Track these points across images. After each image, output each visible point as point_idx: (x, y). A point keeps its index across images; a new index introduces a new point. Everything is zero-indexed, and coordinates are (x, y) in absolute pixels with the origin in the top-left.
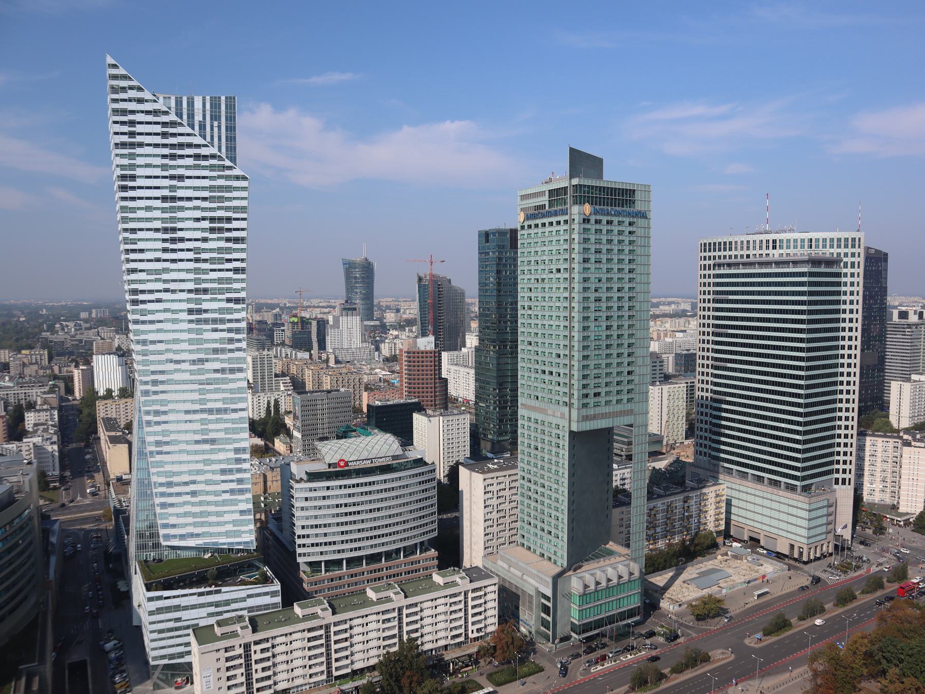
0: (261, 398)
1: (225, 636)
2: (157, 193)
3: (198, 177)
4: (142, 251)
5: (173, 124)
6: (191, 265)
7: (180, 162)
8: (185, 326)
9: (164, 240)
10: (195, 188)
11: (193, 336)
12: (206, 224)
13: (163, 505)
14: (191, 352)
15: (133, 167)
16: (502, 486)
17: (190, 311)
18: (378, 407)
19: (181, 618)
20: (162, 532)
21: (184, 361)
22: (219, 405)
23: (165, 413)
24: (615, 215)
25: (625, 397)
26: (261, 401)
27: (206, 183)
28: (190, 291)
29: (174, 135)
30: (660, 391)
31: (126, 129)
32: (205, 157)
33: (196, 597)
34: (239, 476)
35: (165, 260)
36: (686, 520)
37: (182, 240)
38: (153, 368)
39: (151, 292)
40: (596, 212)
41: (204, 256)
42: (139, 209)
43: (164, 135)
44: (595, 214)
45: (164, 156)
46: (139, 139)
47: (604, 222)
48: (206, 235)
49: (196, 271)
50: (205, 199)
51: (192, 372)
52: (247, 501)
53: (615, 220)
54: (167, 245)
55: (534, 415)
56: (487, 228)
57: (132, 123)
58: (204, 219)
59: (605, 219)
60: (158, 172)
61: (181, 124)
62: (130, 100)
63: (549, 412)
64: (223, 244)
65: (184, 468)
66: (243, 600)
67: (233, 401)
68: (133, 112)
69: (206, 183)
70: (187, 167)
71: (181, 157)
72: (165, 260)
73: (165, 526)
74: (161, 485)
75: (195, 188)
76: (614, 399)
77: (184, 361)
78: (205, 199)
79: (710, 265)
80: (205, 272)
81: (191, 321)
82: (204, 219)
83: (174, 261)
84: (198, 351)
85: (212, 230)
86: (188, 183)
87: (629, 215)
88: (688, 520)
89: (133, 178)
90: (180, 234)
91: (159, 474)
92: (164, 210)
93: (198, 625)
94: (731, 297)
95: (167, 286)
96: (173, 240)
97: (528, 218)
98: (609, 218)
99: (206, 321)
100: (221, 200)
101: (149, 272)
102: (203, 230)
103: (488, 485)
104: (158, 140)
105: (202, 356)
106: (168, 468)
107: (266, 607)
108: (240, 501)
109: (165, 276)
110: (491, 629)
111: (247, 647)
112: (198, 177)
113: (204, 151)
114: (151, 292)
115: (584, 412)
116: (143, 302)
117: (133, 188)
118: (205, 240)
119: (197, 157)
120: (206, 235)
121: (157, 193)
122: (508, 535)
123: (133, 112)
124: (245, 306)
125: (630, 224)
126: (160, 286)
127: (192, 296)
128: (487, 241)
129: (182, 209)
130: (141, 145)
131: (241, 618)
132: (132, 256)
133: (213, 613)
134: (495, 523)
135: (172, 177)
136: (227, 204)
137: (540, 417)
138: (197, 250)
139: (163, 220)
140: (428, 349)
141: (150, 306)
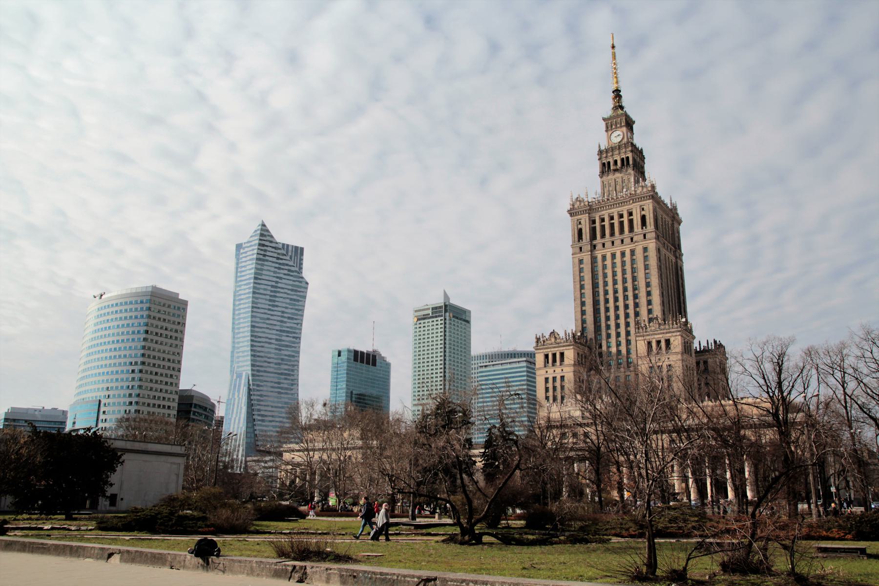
2: (270, 283)
3: (288, 279)
4: (258, 308)
5: (283, 255)
6: (279, 318)
7: (282, 271)
8: (273, 346)
9: (269, 305)
10: (286, 284)
11: (277, 351)
12: (288, 301)
15: (262, 270)
17: (277, 340)
21: (272, 363)
22: (286, 386)
23: (262, 386)
27: (291, 283)
28: (277, 330)
29: (282, 259)
31: (262, 253)
32: (293, 271)
35: (269, 314)
37: (277, 306)
39: (261, 328)
40: (454, 317)
42: (262, 289)
43: (278, 258)
45: (276, 268)
46: (267, 258)
48: (287, 306)
49: (282, 321)
50: (289, 289)
54: (270, 307)
57: (265, 251)
58: (287, 298)
59: (456, 320)
60: (272, 274)
62: (267, 241)
64: (293, 311)
65: (269, 414)
68: (267, 246)
69: (291, 283)
70: (285, 274)
71: (283, 269)
72: (269, 314)
74: (259, 420)
75: (286, 284)
77: (272, 363)
78: (289, 289)
79: (475, 368)
81: (276, 345)
82: (287, 298)
83: (272, 315)
86: (283, 281)
89: (261, 274)
90: (276, 303)
91: (259, 415)
92: (271, 291)
94: (490, 377)
95: (268, 326)
97: (418, 320)
100: (296, 291)
101: (261, 318)
102: (286, 303)
104: (274, 260)
106: (262, 413)
109: (267, 322)
112: (288, 279)
113: (293, 269)
114: (261, 328)
116: (258, 332)
117: (260, 279)
118: (286, 308)
119: (289, 270)
120: (287, 306)
121: (270, 283)
123: (267, 246)
126: (265, 326)
127: (278, 333)
129: (279, 292)
130: (267, 261)
132: (255, 310)
135: (277, 277)
136: (298, 293)
138: (283, 312)
139: (271, 296)
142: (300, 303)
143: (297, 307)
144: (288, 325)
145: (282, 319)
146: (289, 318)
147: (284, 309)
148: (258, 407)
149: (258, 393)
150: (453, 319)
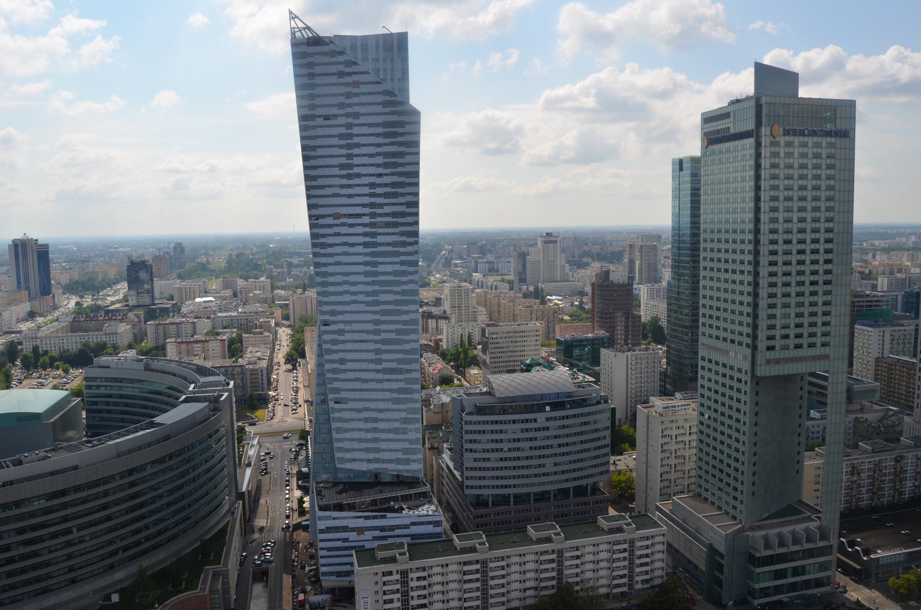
0: (456, 328)
1: (385, 561)
5: (350, 63)
13: (339, 430)
14: (367, 284)
16: (681, 431)
18: (566, 342)
19: (348, 539)
20: (338, 455)
24: (809, 135)
25: (818, 340)
26: (456, 332)
28: (365, 225)
30: (881, 334)
33: (362, 520)
34: (409, 405)
36: (898, 483)
37: (358, 175)
38: (332, 298)
40: (787, 133)
41: (379, 190)
44: (784, 135)
47: (796, 144)
51: (367, 304)
52: (417, 430)
53: (811, 140)
55: (715, 357)
56: (681, 156)
58: (378, 154)
59: (797, 140)
61: (355, 63)
63: (732, 354)
64: (395, 179)
66: (406, 527)
67: (406, 332)
73: (341, 450)
76: (805, 341)
80: (381, 206)
81: (365, 254)
82: (378, 154)
84: (373, 283)
85: (386, 165)
86: (363, 120)
87: (828, 134)
88: (901, 482)
93: (363, 546)
96: (349, 177)
98: (801, 139)
99: (381, 254)
102: (378, 165)
103: (666, 429)
105: (377, 288)
107: (429, 536)
108: (411, 430)
110: (658, 582)
111: (404, 574)
115: (771, 355)
122: (686, 483)
124: (416, 239)
125: (830, 145)
127: (367, 229)
128: (681, 169)
131: (401, 545)
132: (314, 192)
133: (378, 537)
134: (673, 469)
135: (348, 115)
137: (722, 360)
138: (372, 185)
140: (621, 282)
141: (330, 240)
142: (408, 159)
143: (400, 169)
144: (387, 210)
145: (373, 200)
146: (386, 195)
147: (373, 180)
148: (336, 385)
149: (336, 357)
150: (782, 140)
